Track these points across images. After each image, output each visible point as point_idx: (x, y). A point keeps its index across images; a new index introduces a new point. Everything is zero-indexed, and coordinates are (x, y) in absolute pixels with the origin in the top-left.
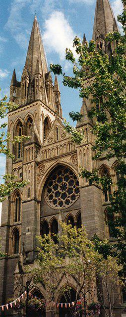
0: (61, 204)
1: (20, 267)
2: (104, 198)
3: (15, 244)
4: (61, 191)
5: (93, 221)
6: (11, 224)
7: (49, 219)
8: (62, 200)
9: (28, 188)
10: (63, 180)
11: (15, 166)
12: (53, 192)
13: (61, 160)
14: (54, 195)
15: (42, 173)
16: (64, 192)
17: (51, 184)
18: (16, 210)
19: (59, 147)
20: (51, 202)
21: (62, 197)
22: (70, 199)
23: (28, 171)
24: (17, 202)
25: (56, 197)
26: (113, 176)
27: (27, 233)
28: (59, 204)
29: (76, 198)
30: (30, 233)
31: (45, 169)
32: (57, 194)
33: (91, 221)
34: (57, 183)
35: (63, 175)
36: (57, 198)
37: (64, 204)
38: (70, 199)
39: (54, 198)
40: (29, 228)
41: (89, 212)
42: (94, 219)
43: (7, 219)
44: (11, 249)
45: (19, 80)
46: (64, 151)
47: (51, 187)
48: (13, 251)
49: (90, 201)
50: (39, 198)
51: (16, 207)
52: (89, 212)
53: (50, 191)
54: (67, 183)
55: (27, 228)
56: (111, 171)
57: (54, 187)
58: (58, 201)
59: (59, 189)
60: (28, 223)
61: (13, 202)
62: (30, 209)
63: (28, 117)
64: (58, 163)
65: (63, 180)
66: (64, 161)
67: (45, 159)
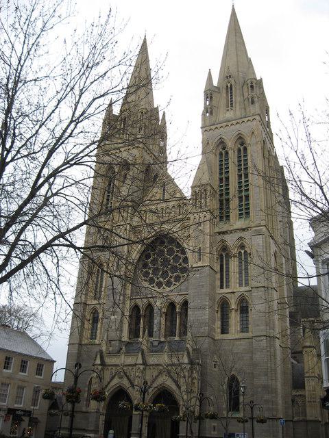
1: (102, 358)
2: (219, 284)
6: (89, 302)
8: (161, 279)
24: (98, 275)
29: (182, 280)
32: (156, 271)
48: (89, 336)
53: (145, 266)
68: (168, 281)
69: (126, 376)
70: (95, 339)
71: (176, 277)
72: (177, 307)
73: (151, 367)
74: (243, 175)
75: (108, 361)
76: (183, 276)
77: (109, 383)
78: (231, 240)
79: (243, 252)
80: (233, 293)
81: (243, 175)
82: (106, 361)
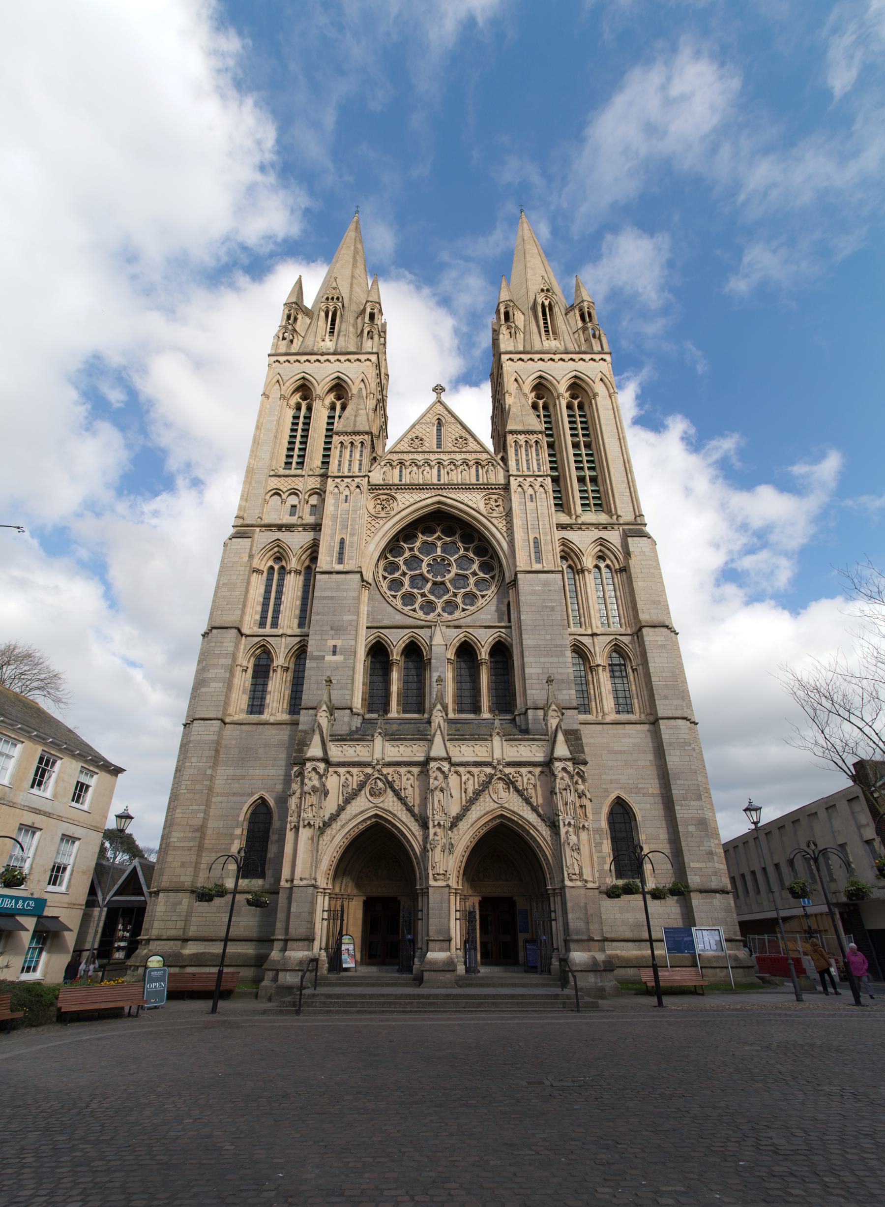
0: (429, 607)
3: (254, 685)
4: (430, 576)
5: (561, 660)
7: (397, 641)
8: (432, 598)
9: (337, 540)
10: (439, 550)
11: (274, 483)
12: (404, 574)
13: (450, 495)
14: (406, 581)
15: (383, 514)
16: (439, 579)
17: (398, 551)
18: (266, 598)
19: (446, 463)
20: (395, 597)
21: (432, 592)
22: (459, 600)
23: (343, 497)
24: (269, 580)
25: (412, 587)
26: (590, 572)
27: (329, 658)
28: (422, 608)
29: (480, 602)
30: (339, 658)
31: (397, 507)
33: (555, 660)
34: (417, 553)
35: (439, 538)
36: (415, 591)
37: (439, 610)
38: (459, 600)
39: (407, 587)
40: (339, 643)
41: (548, 637)
42: (564, 655)
43: (239, 612)
44: (239, 700)
45: (309, 301)
46: (470, 476)
47: (400, 560)
49: (552, 609)
50: (369, 577)
51: (268, 592)
52: (548, 637)
54: (451, 559)
55: (331, 643)
56: (584, 559)
57: (406, 562)
58: (420, 600)
59: (425, 568)
60: (338, 629)
61: (257, 571)
62: (345, 594)
63: (334, 383)
64: (439, 502)
65: (439, 550)
66: (458, 499)
67: (397, 481)
68: (448, 603)
69: (394, 790)
70: (261, 712)
71: (466, 595)
72: (483, 651)
73: (461, 770)
74: (582, 444)
75: (336, 752)
76: (483, 596)
77: (341, 809)
78: (584, 540)
79: (602, 565)
80: (593, 635)
81: (582, 444)
82: (330, 753)
